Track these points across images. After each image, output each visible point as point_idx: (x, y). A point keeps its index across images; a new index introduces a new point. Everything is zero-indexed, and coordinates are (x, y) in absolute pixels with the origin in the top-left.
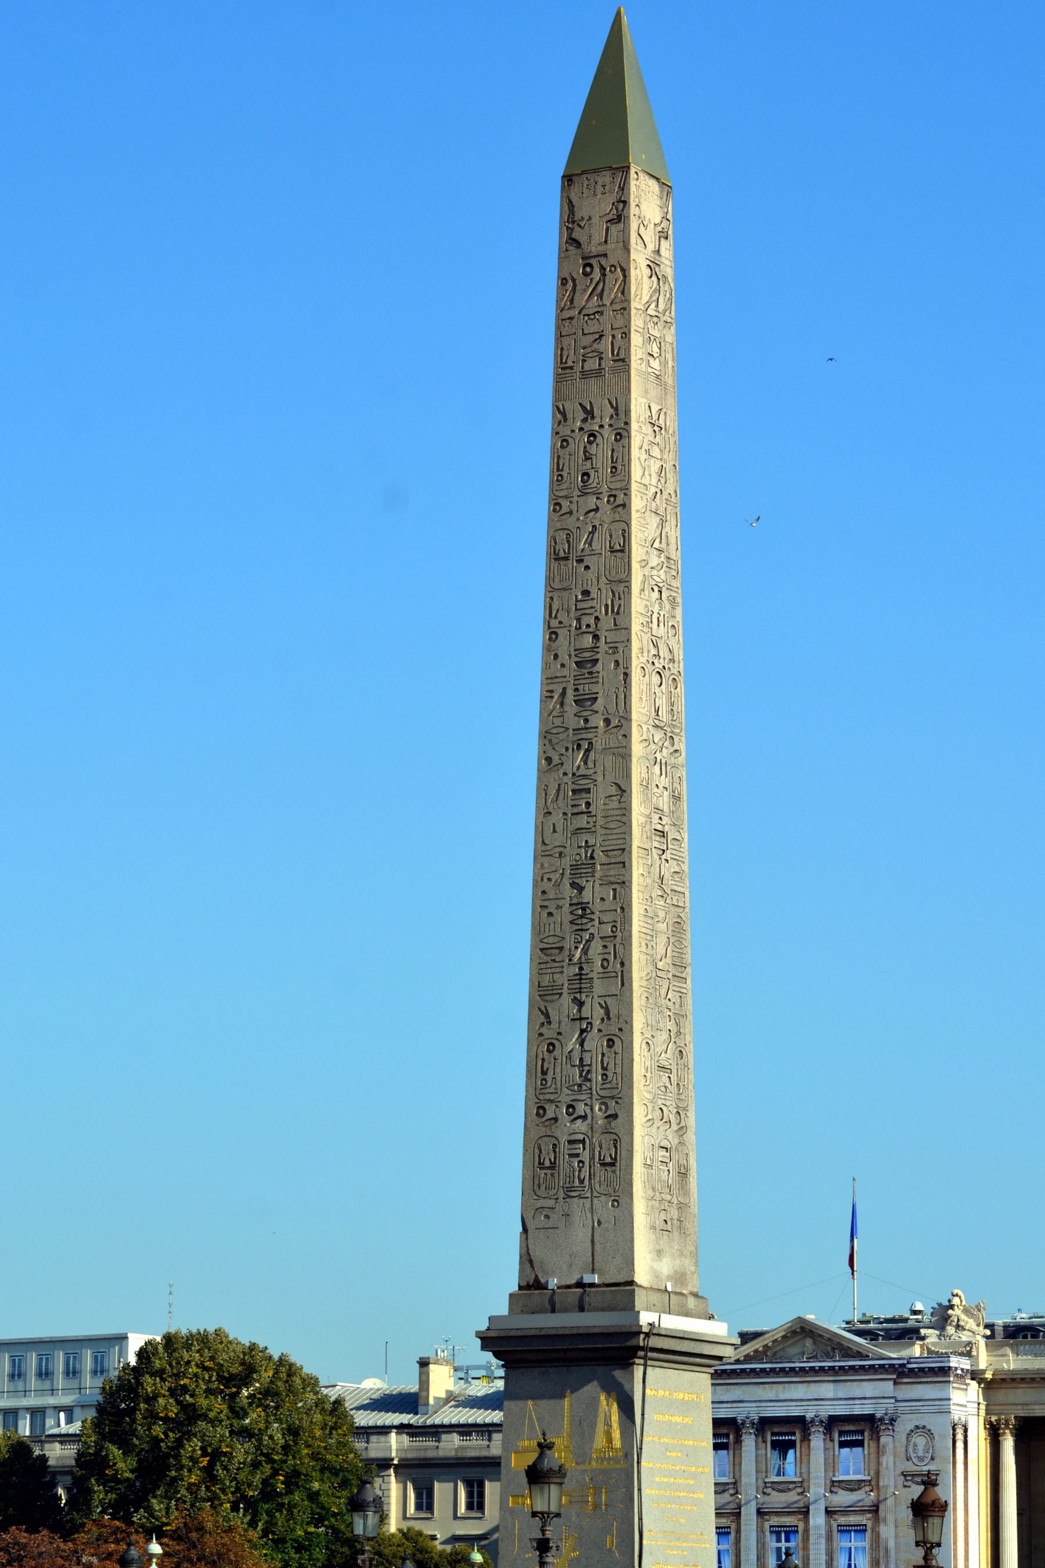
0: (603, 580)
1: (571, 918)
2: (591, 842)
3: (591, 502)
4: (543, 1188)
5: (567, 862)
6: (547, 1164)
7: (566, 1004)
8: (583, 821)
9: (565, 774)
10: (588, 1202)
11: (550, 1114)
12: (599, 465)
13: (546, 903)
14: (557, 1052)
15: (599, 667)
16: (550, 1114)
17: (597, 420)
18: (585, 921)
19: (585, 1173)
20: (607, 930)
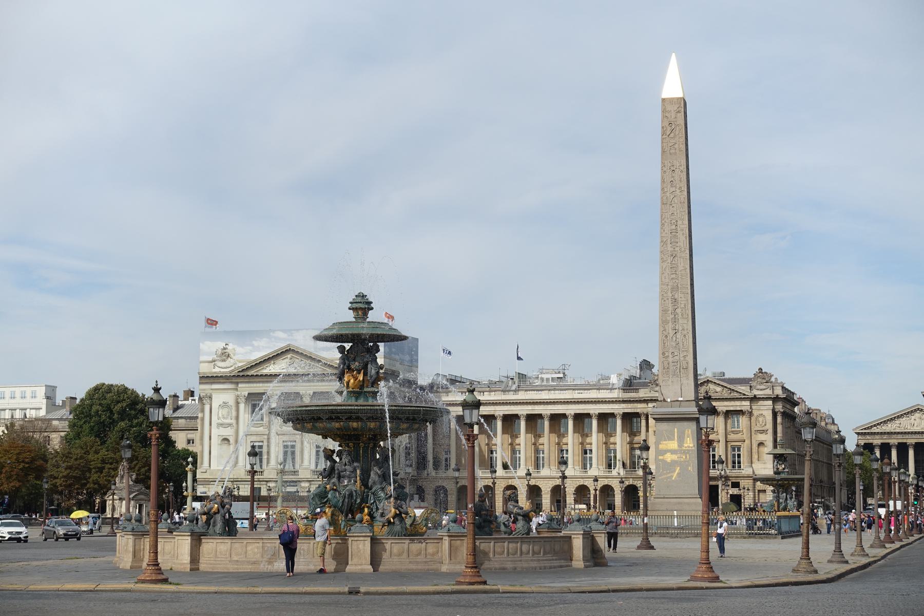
3: (674, 189)
8: (674, 276)
20: (683, 306)
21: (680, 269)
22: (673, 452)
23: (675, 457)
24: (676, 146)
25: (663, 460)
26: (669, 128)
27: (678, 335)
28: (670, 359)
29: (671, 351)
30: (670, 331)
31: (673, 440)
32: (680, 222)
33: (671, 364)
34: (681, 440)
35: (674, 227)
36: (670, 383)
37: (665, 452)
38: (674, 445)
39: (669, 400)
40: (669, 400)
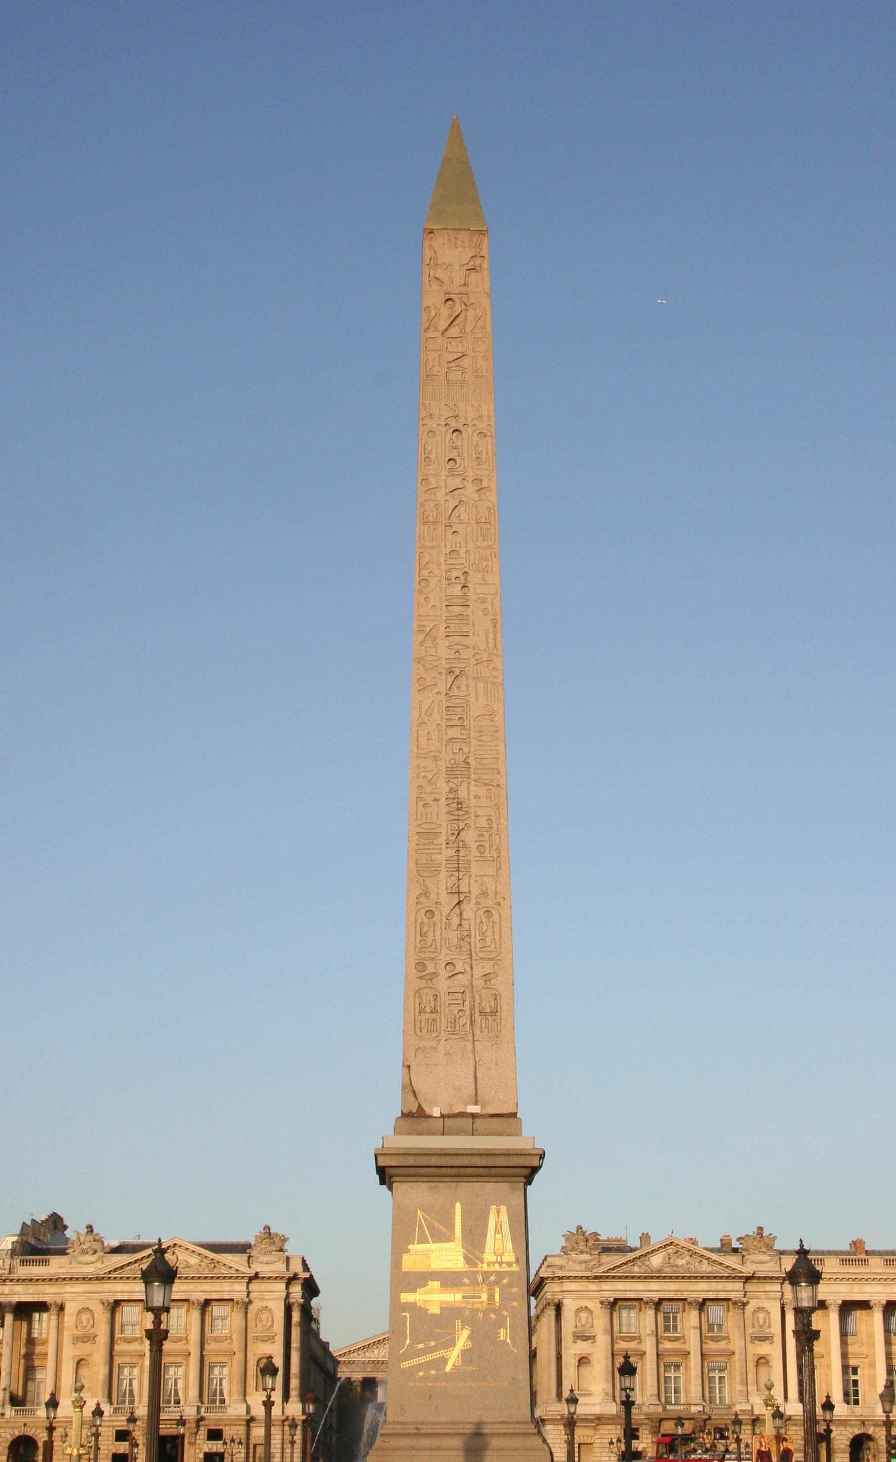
0: (471, 545)
1: (447, 809)
2: (466, 750)
3: (457, 482)
4: (424, 1031)
5: (442, 765)
6: (428, 1010)
7: (445, 880)
8: (455, 733)
9: (438, 693)
10: (470, 1047)
11: (430, 969)
12: (465, 455)
13: (423, 796)
14: (436, 918)
15: (469, 612)
16: (430, 969)
17: (463, 420)
18: (461, 813)
19: (466, 1019)
20: (482, 822)
23: (454, 1297)
24: (466, 363)
27: (469, 911)
28: (443, 984)
29: (443, 958)
30: (444, 897)
31: (449, 1239)
32: (474, 579)
33: (444, 999)
34: (474, 1241)
35: (457, 590)
37: (419, 1280)
38: (448, 1256)
39: (436, 1112)
40: (436, 1112)
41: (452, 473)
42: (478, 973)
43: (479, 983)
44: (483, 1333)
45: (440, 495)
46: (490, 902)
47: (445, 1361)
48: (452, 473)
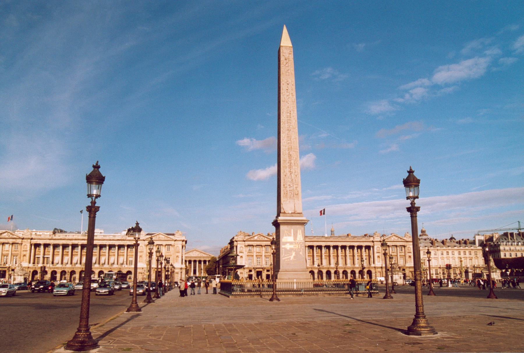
3: (288, 94)
8: (289, 142)
21: (293, 138)
22: (291, 243)
24: (289, 71)
25: (284, 248)
26: (285, 62)
27: (293, 175)
28: (288, 189)
29: (288, 184)
30: (288, 173)
31: (291, 236)
32: (292, 112)
33: (288, 192)
35: (289, 114)
36: (288, 202)
37: (286, 243)
38: (291, 239)
41: (287, 92)
42: (295, 186)
43: (295, 189)
44: (297, 253)
45: (285, 96)
46: (296, 174)
47: (290, 258)
48: (287, 92)
